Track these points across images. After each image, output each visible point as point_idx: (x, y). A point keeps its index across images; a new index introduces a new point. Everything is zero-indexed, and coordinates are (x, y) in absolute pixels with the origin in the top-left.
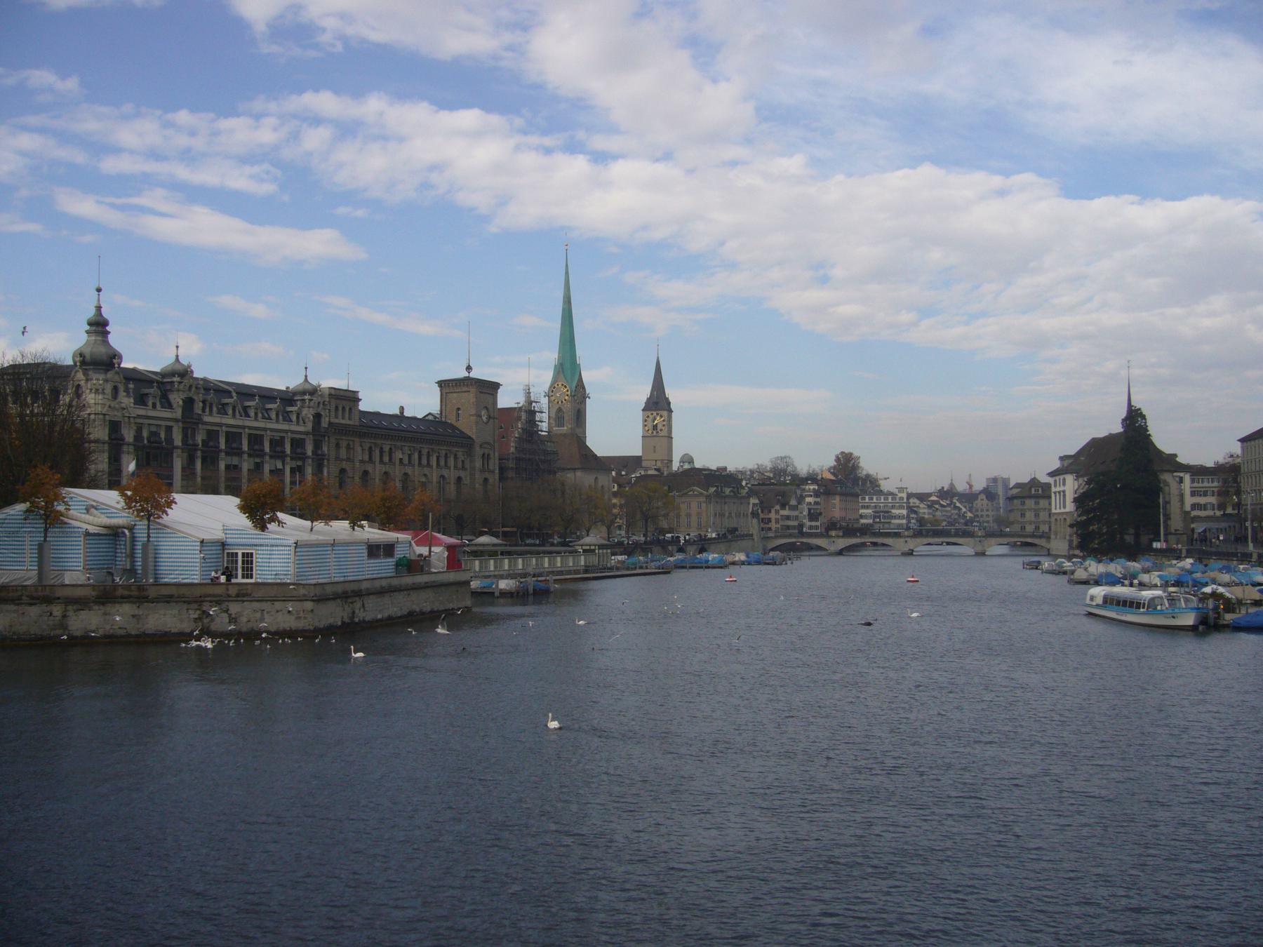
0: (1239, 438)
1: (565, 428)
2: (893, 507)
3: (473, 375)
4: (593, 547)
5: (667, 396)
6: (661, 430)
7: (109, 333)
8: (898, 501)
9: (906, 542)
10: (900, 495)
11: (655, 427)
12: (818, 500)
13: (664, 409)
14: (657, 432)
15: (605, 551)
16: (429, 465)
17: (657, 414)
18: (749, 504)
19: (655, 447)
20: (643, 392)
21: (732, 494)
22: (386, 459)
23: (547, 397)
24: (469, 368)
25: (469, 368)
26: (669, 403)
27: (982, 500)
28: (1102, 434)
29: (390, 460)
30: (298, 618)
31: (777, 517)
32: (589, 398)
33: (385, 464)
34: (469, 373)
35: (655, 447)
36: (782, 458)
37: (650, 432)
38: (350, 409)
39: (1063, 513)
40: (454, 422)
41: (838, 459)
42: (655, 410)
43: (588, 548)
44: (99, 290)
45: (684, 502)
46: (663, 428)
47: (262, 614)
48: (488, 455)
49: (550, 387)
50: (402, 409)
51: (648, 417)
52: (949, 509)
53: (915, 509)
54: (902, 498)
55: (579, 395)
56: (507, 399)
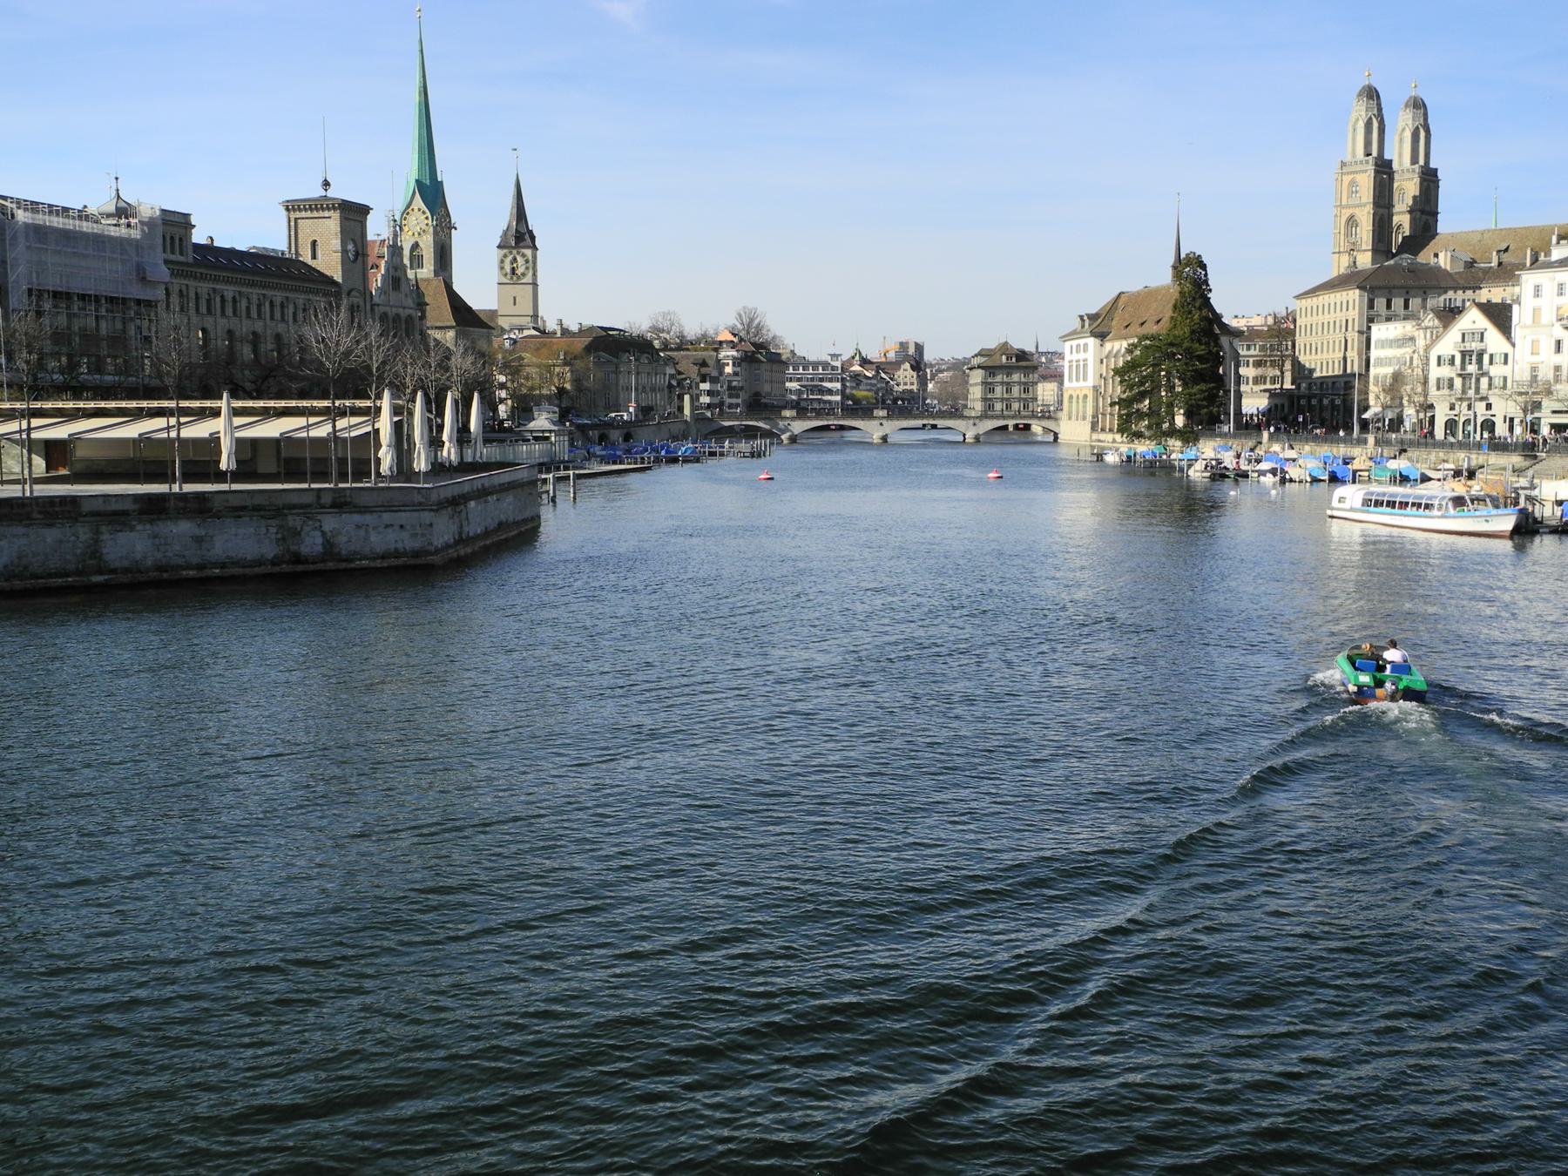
1: (425, 270)
6: (523, 274)
12: (738, 369)
13: (528, 247)
16: (283, 319)
22: (229, 311)
24: (326, 184)
25: (326, 184)
26: (533, 238)
28: (1133, 286)
29: (235, 313)
30: (414, 535)
33: (228, 317)
36: (664, 315)
38: (181, 240)
39: (1081, 389)
40: (309, 260)
47: (367, 531)
51: (505, 256)
52: (874, 382)
54: (834, 368)
56: (377, 229)
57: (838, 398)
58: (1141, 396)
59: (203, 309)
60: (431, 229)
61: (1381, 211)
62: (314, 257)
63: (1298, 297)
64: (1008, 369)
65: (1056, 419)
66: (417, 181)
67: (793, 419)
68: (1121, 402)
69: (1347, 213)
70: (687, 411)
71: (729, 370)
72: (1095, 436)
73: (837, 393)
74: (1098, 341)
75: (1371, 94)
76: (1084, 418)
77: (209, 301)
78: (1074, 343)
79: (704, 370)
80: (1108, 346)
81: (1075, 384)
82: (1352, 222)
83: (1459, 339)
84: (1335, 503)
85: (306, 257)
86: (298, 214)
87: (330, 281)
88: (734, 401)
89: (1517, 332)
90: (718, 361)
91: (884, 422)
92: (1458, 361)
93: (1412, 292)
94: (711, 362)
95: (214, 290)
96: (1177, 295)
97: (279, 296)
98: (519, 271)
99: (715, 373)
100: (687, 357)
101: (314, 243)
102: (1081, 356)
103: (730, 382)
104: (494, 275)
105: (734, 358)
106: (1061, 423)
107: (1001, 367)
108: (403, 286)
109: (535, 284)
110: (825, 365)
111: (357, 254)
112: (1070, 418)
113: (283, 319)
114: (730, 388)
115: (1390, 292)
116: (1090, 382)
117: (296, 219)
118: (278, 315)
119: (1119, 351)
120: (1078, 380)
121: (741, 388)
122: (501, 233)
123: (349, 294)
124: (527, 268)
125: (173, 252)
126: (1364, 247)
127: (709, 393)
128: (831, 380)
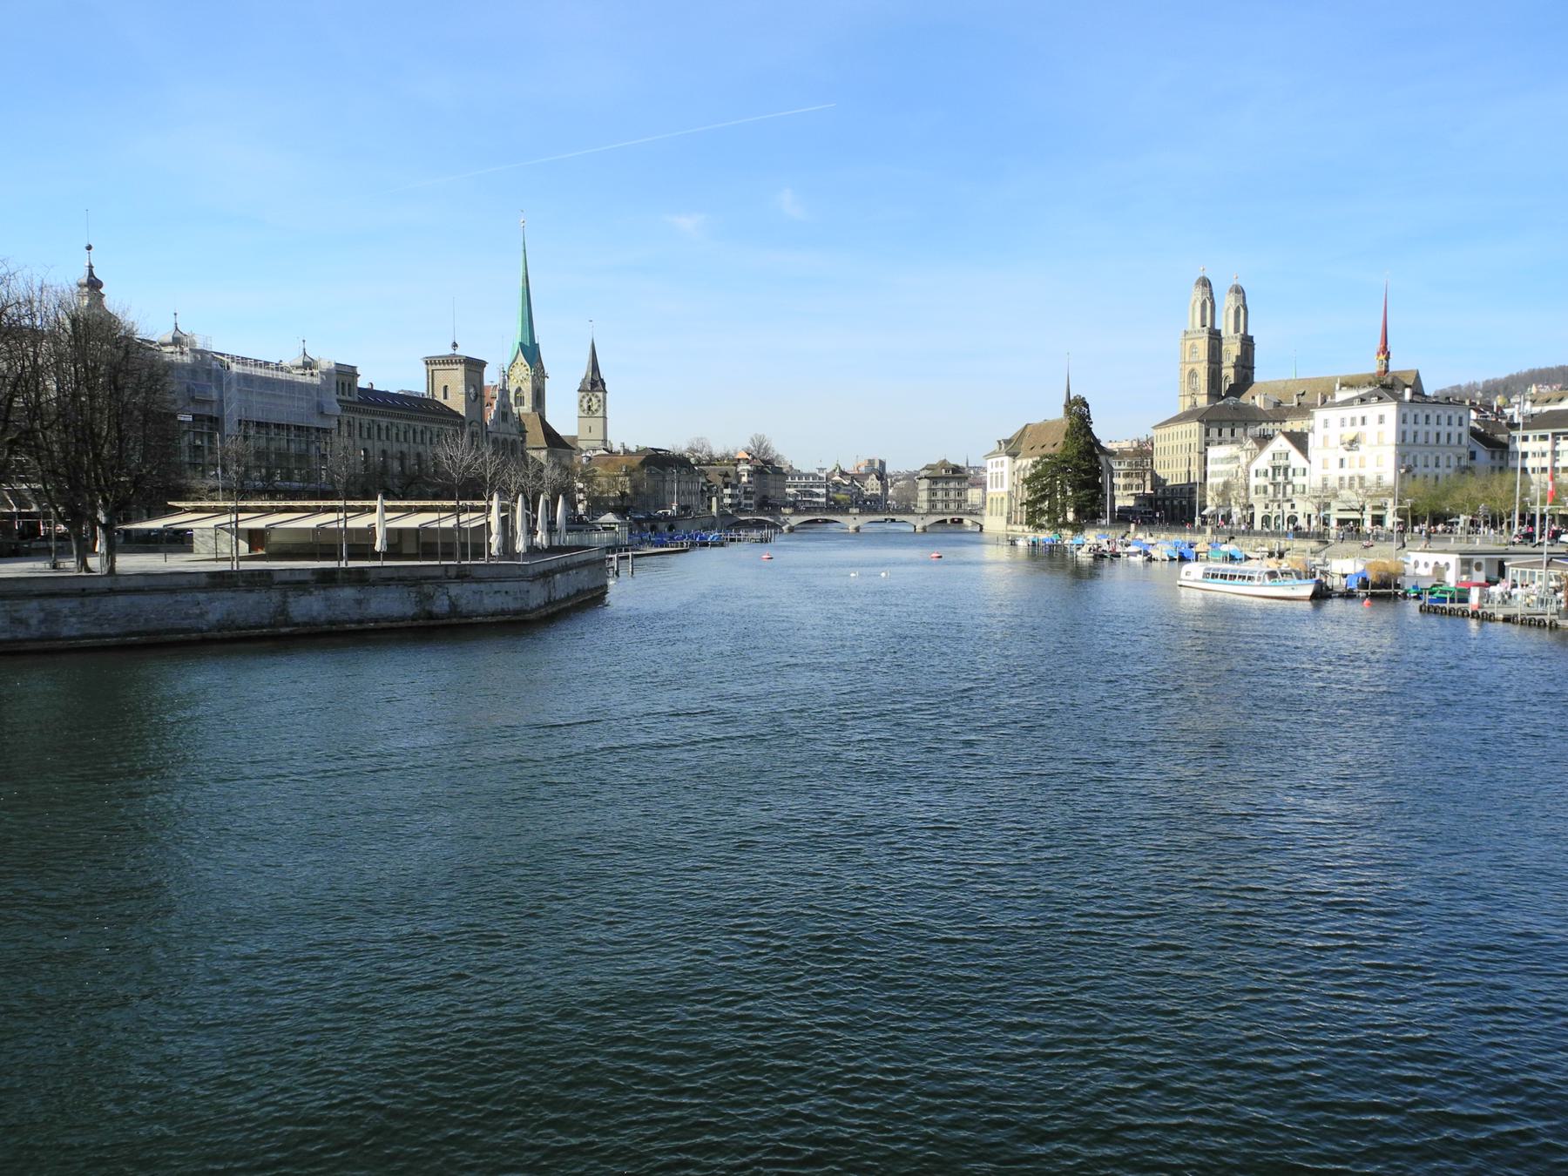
1: (525, 407)
7: (103, 295)
13: (600, 391)
16: (422, 442)
22: (383, 436)
24: (455, 345)
25: (455, 345)
26: (603, 384)
28: (1036, 419)
29: (387, 438)
38: (349, 385)
39: (999, 493)
40: (441, 400)
44: (89, 248)
51: (583, 397)
52: (850, 488)
54: (820, 478)
56: (491, 377)
57: (824, 500)
58: (1043, 498)
59: (365, 434)
61: (1213, 366)
62: (445, 397)
63: (1154, 428)
64: (947, 479)
65: (981, 515)
66: (521, 344)
67: (791, 514)
68: (1028, 503)
69: (1189, 368)
70: (714, 509)
71: (744, 479)
72: (1009, 527)
74: (1011, 459)
75: (1205, 283)
76: (1002, 514)
77: (369, 429)
78: (994, 460)
79: (727, 479)
80: (1019, 462)
81: (994, 490)
82: (1193, 374)
84: (1183, 575)
85: (440, 397)
86: (434, 367)
87: (457, 415)
88: (748, 502)
90: (737, 473)
91: (857, 517)
92: (1270, 473)
93: (1237, 424)
94: (732, 474)
95: (373, 421)
96: (1068, 426)
97: (419, 426)
98: (593, 408)
99: (734, 482)
100: (715, 470)
102: (999, 469)
103: (745, 488)
104: (575, 411)
105: (749, 471)
107: (941, 478)
108: (509, 417)
109: (605, 417)
110: (814, 476)
111: (476, 396)
112: (991, 514)
113: (422, 442)
114: (745, 492)
116: (1006, 488)
118: (419, 439)
119: (1026, 466)
120: (997, 486)
121: (754, 493)
123: (470, 424)
125: (343, 394)
127: (731, 496)
128: (818, 487)
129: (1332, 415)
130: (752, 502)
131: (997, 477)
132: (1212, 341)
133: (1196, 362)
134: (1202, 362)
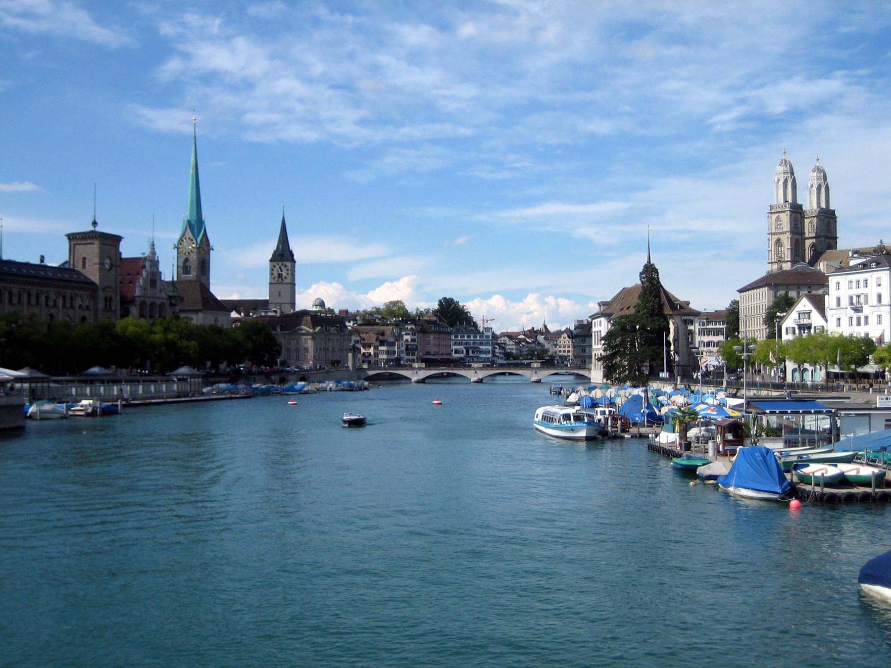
0: (738, 289)
1: (191, 275)
2: (481, 344)
3: (99, 229)
4: (185, 377)
5: (291, 249)
8: (485, 338)
9: (476, 372)
10: (486, 334)
11: (280, 276)
12: (415, 337)
14: (282, 280)
15: (196, 380)
17: (282, 264)
18: (351, 340)
19: (280, 293)
20: (272, 246)
21: (335, 332)
23: (176, 249)
24: (95, 223)
25: (95, 223)
26: (292, 255)
27: (565, 338)
31: (376, 351)
32: (213, 250)
34: (95, 227)
35: (280, 293)
37: (276, 279)
41: (441, 304)
42: (280, 261)
43: (181, 377)
45: (293, 339)
46: (287, 276)
48: (111, 298)
49: (179, 241)
50: (42, 259)
52: (533, 345)
53: (503, 345)
54: (487, 337)
55: (205, 248)
57: (490, 356)
60: (196, 250)
63: (740, 291)
66: (189, 222)
69: (775, 237)
70: (350, 364)
73: (489, 352)
82: (778, 242)
83: (797, 317)
85: (79, 267)
86: (75, 242)
87: (94, 284)
88: (410, 357)
89: (828, 313)
92: (797, 331)
93: (790, 287)
95: (24, 289)
99: (391, 340)
101: (84, 259)
106: (592, 371)
109: (293, 284)
113: (37, 304)
114: (407, 349)
115: (787, 287)
117: (75, 245)
122: (272, 253)
124: (288, 274)
126: (786, 259)
127: (387, 353)
128: (486, 344)
129: (843, 279)
130: (415, 357)
131: (598, 335)
132: (794, 215)
133: (780, 233)
134: (785, 233)
